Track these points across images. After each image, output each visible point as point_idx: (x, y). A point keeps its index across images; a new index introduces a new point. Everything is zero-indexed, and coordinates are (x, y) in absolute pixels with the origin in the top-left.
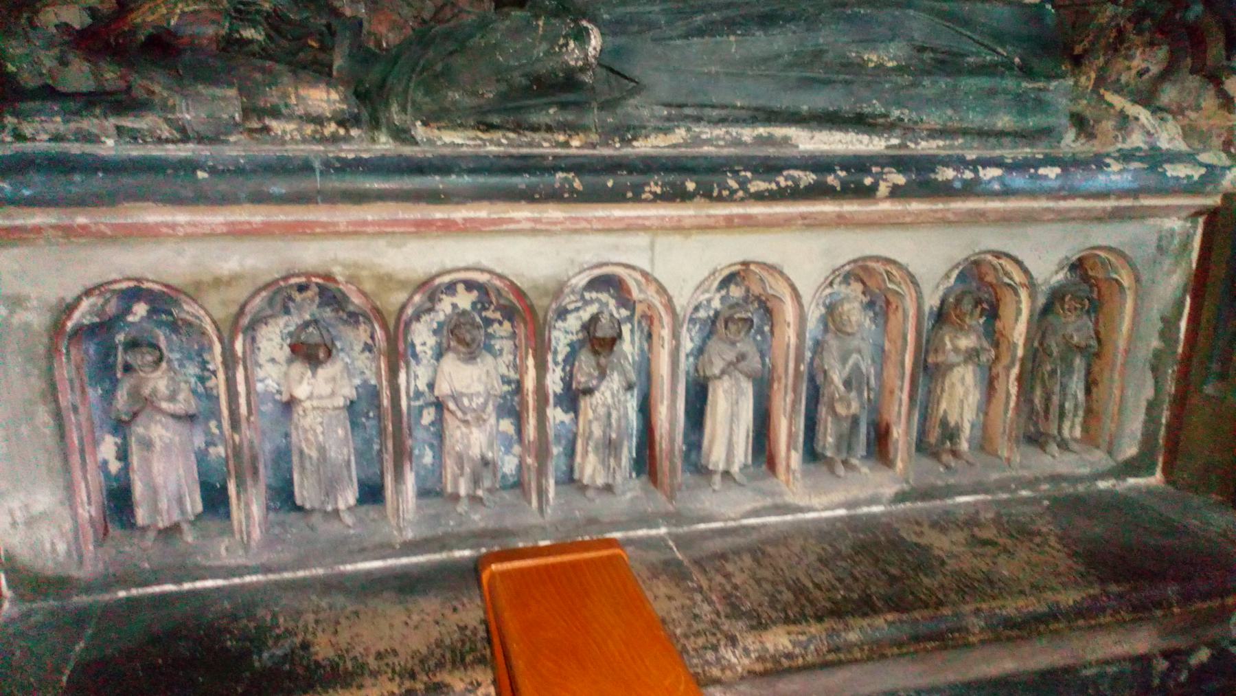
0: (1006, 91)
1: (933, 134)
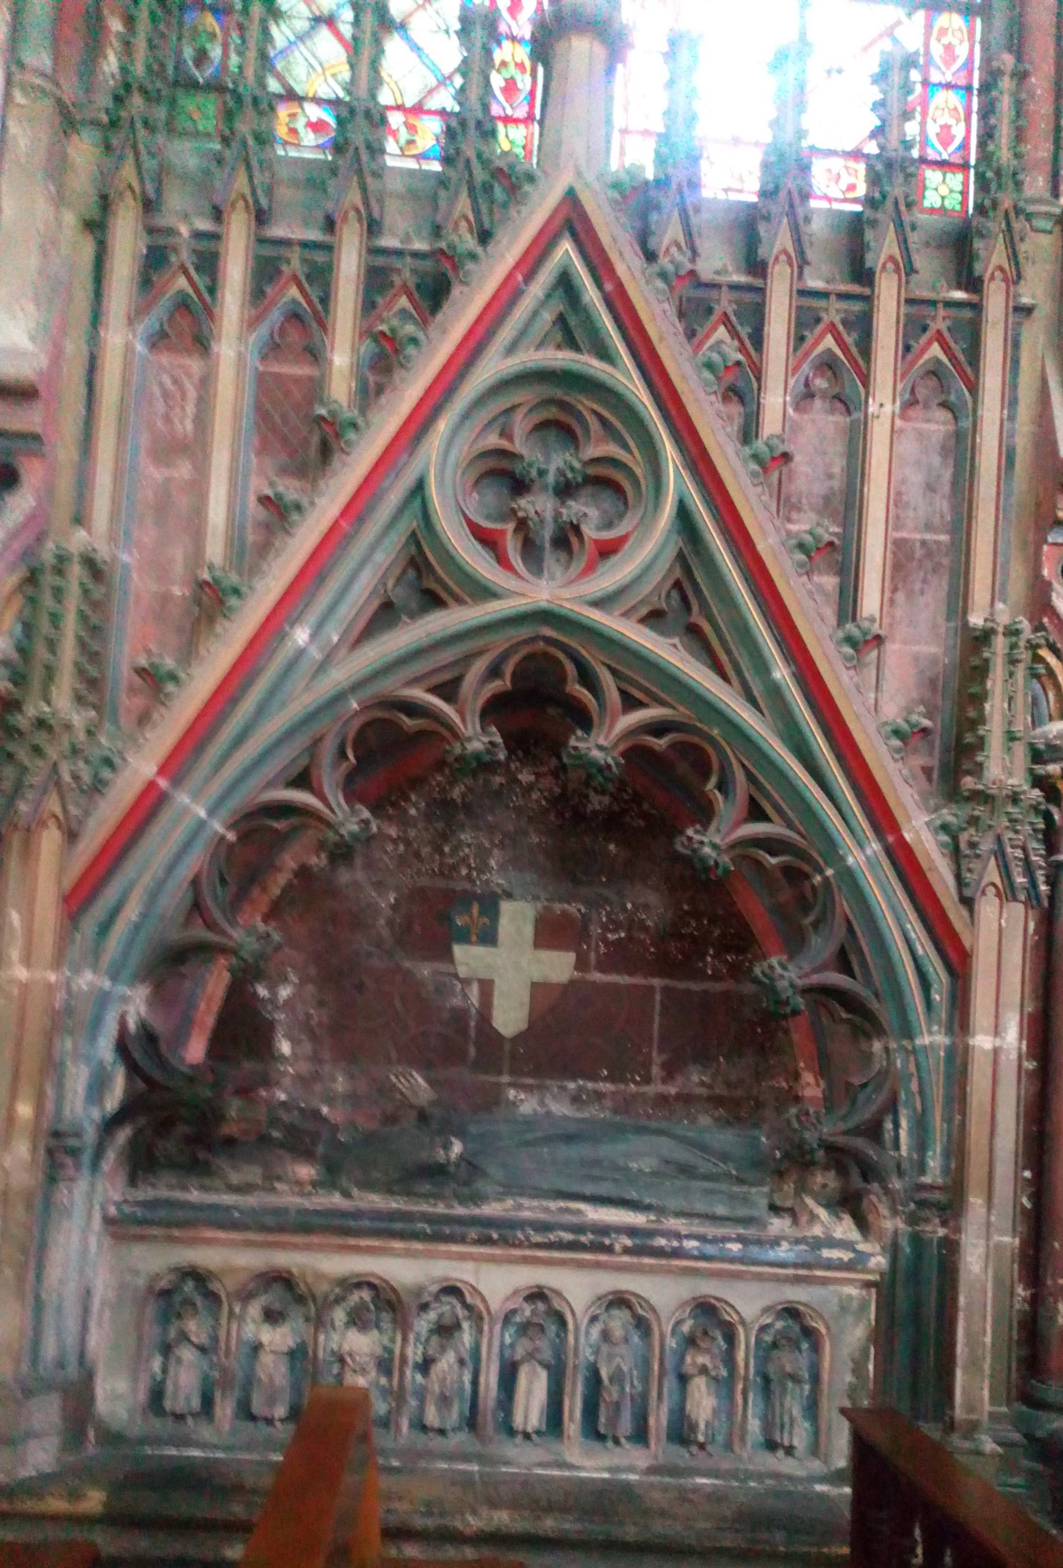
0: (721, 1192)
1: (679, 1214)
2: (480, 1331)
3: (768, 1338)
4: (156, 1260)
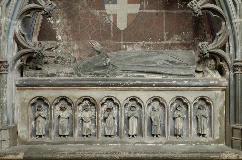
3: (197, 107)
4: (30, 95)
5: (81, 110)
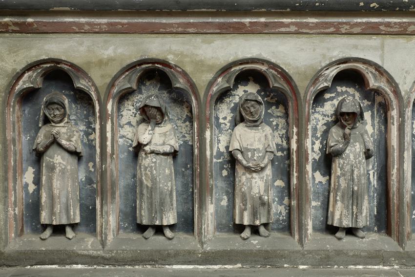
2: (385, 121)
5: (226, 122)
